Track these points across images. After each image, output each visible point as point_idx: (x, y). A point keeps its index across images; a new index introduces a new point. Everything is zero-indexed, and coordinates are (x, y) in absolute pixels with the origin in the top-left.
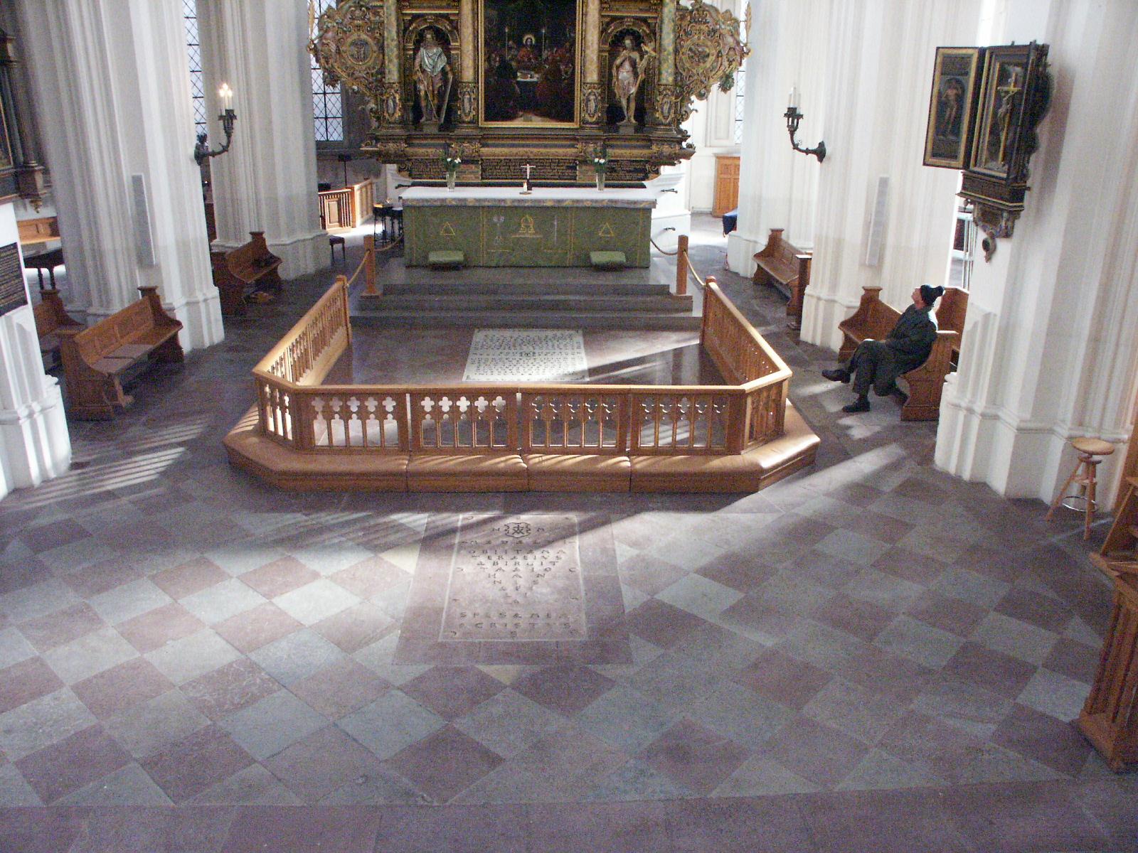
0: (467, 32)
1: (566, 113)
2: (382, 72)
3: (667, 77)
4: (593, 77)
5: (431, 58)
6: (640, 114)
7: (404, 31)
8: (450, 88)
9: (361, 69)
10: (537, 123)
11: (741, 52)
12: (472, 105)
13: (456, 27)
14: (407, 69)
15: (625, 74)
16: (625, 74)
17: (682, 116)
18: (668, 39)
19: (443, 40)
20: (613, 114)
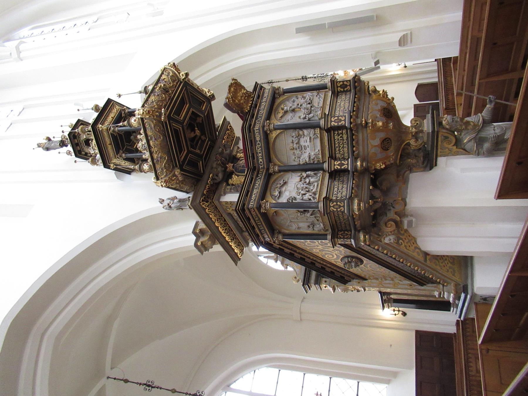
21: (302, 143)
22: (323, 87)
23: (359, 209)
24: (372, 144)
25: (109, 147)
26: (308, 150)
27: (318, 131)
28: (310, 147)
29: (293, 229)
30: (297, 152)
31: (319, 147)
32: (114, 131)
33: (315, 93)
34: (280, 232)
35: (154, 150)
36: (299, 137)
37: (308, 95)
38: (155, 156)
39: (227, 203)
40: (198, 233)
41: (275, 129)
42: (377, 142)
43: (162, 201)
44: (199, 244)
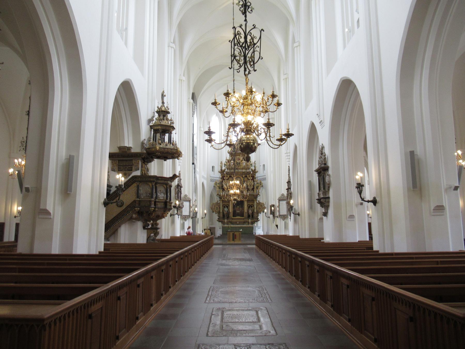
0: (230, 206)
1: (243, 216)
2: (220, 211)
3: (255, 211)
4: (246, 211)
5: (226, 209)
6: (252, 216)
7: (223, 206)
8: (228, 213)
9: (217, 211)
10: (239, 217)
11: (265, 208)
12: (231, 215)
13: (229, 206)
14: (223, 210)
15: (250, 211)
16: (250, 211)
17: (258, 216)
18: (255, 206)
19: (227, 207)
20: (249, 216)
24: (159, 213)
29: (141, 188)
31: (161, 198)
36: (164, 193)
39: (139, 162)
40: (129, 148)
42: (159, 214)
43: (145, 140)
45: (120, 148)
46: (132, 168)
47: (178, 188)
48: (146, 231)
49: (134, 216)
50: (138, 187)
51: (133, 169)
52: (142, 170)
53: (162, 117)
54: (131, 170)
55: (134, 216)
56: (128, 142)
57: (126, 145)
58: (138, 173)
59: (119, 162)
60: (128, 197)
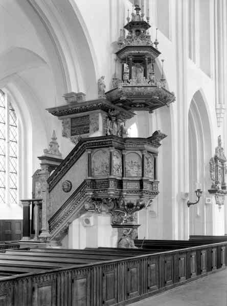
21: (135, 167)
22: (155, 177)
23: (110, 194)
25: (137, 52)
26: (132, 170)
27: (141, 175)
28: (134, 172)
30: (130, 164)
31: (133, 175)
32: (146, 57)
33: (153, 173)
34: (92, 152)
35: (139, 89)
36: (138, 166)
37: (153, 170)
38: (136, 88)
39: (98, 117)
40: (79, 96)
41: (143, 156)
42: (132, 202)
43: (103, 78)
44: (74, 95)
45: (68, 96)
46: (89, 128)
47: (216, 162)
48: (116, 229)
49: (87, 206)
50: (89, 156)
51: (91, 127)
52: (105, 131)
53: (134, 34)
54: (88, 132)
55: (87, 206)
56: (77, 85)
57: (74, 90)
58: (99, 134)
59: (72, 121)
60: (77, 175)
